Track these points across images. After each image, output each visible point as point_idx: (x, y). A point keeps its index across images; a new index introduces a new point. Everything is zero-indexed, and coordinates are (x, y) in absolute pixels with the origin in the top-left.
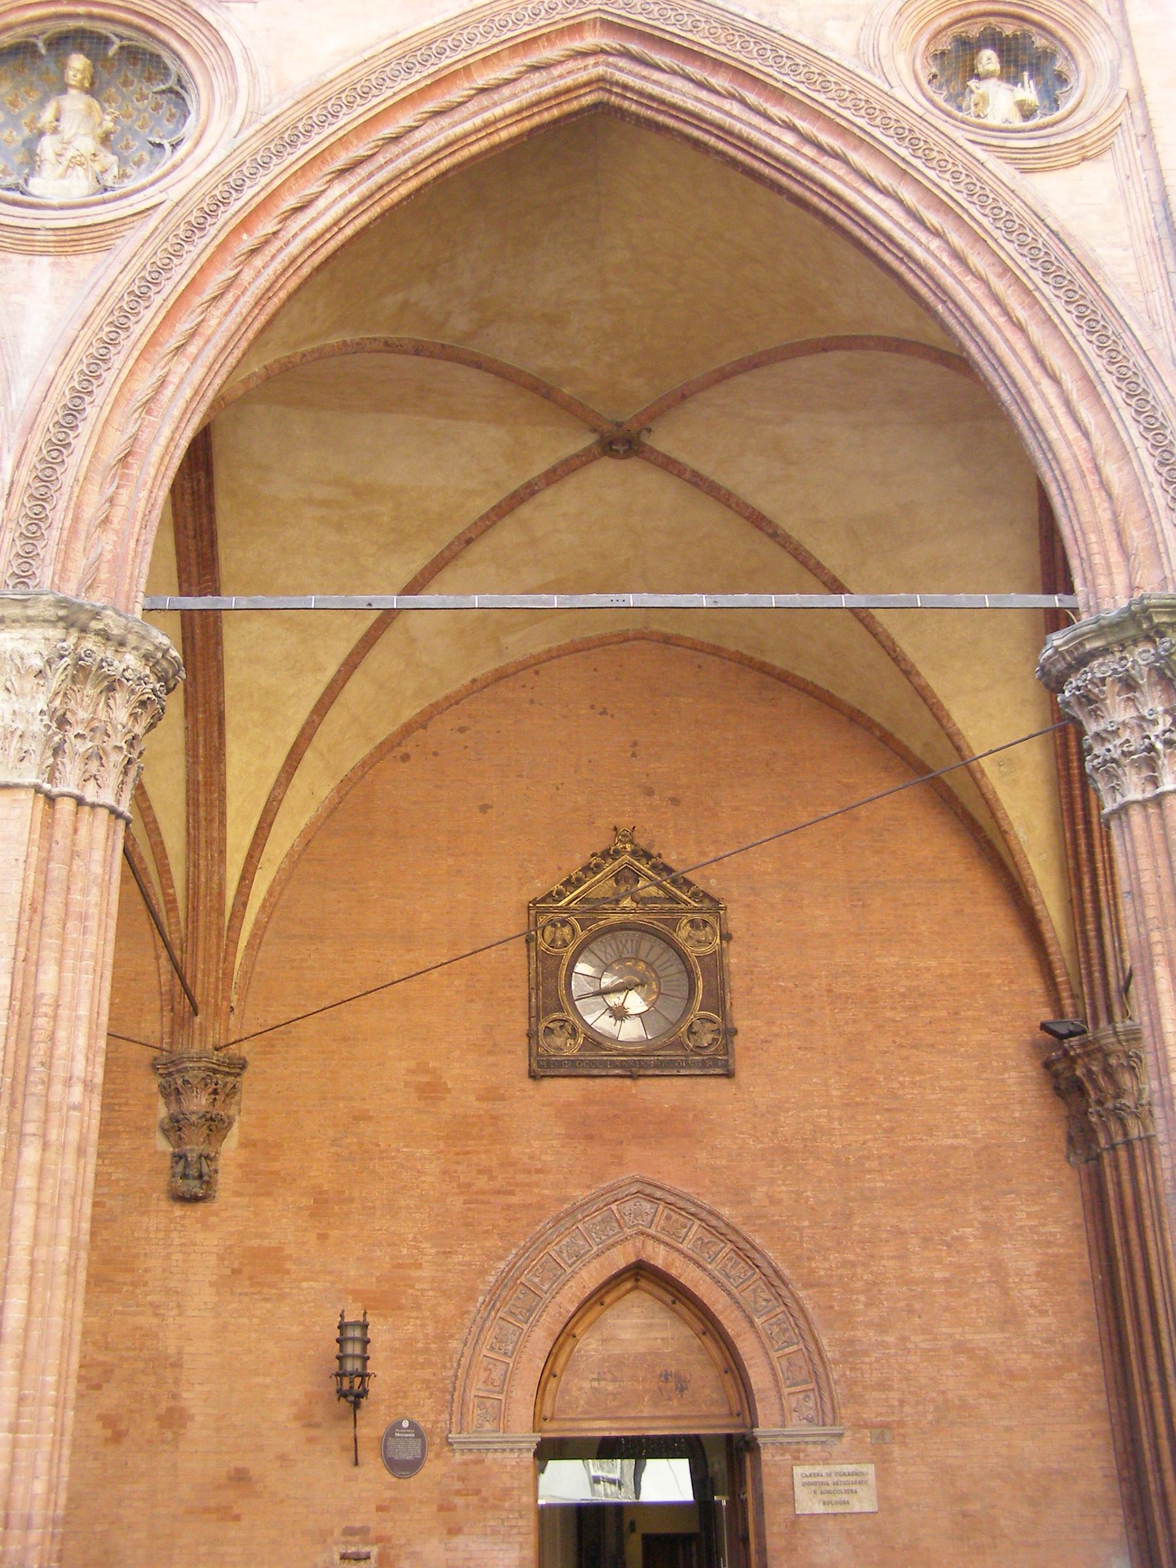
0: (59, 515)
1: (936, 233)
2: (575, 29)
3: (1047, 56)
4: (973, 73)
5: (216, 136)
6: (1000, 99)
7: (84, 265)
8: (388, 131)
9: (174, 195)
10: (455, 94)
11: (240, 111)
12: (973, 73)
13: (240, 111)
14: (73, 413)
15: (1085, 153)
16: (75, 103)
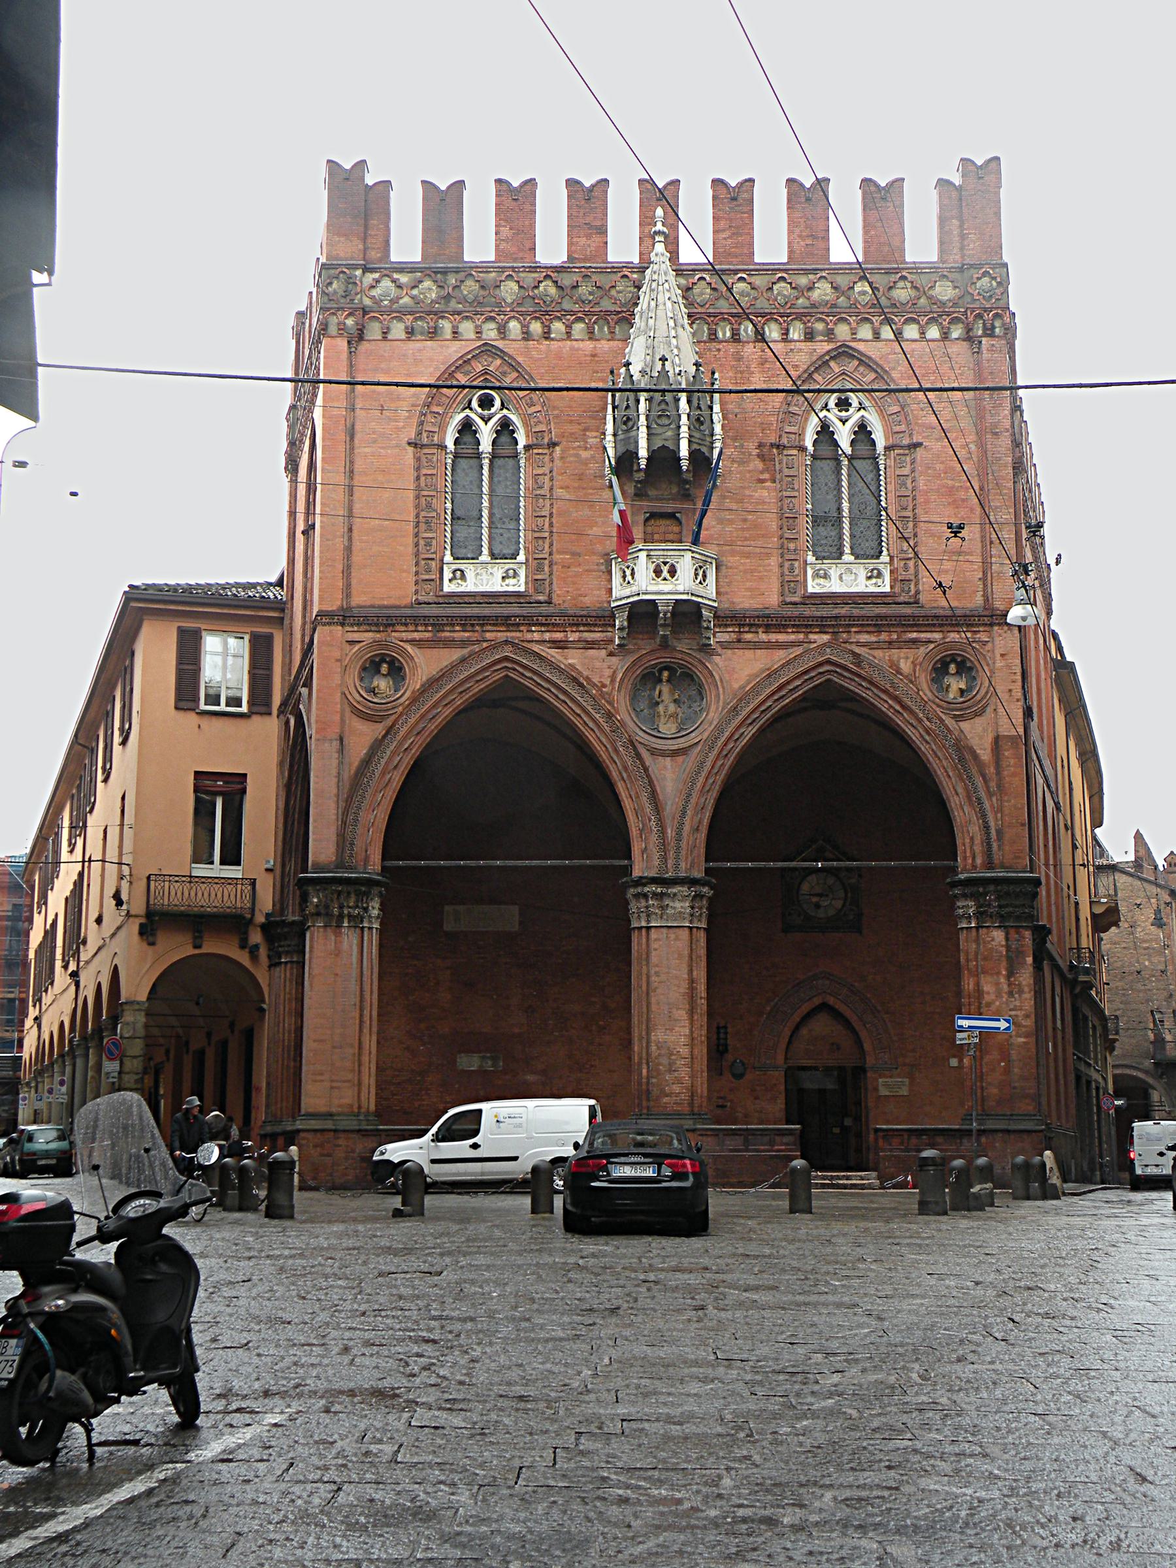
0: (684, 844)
1: (927, 742)
2: (820, 664)
3: (971, 669)
4: (947, 673)
5: (713, 713)
6: (956, 684)
7: (680, 759)
8: (763, 708)
9: (705, 737)
10: (783, 693)
11: (721, 703)
12: (947, 673)
13: (721, 703)
14: (684, 813)
15: (979, 713)
16: (665, 688)
